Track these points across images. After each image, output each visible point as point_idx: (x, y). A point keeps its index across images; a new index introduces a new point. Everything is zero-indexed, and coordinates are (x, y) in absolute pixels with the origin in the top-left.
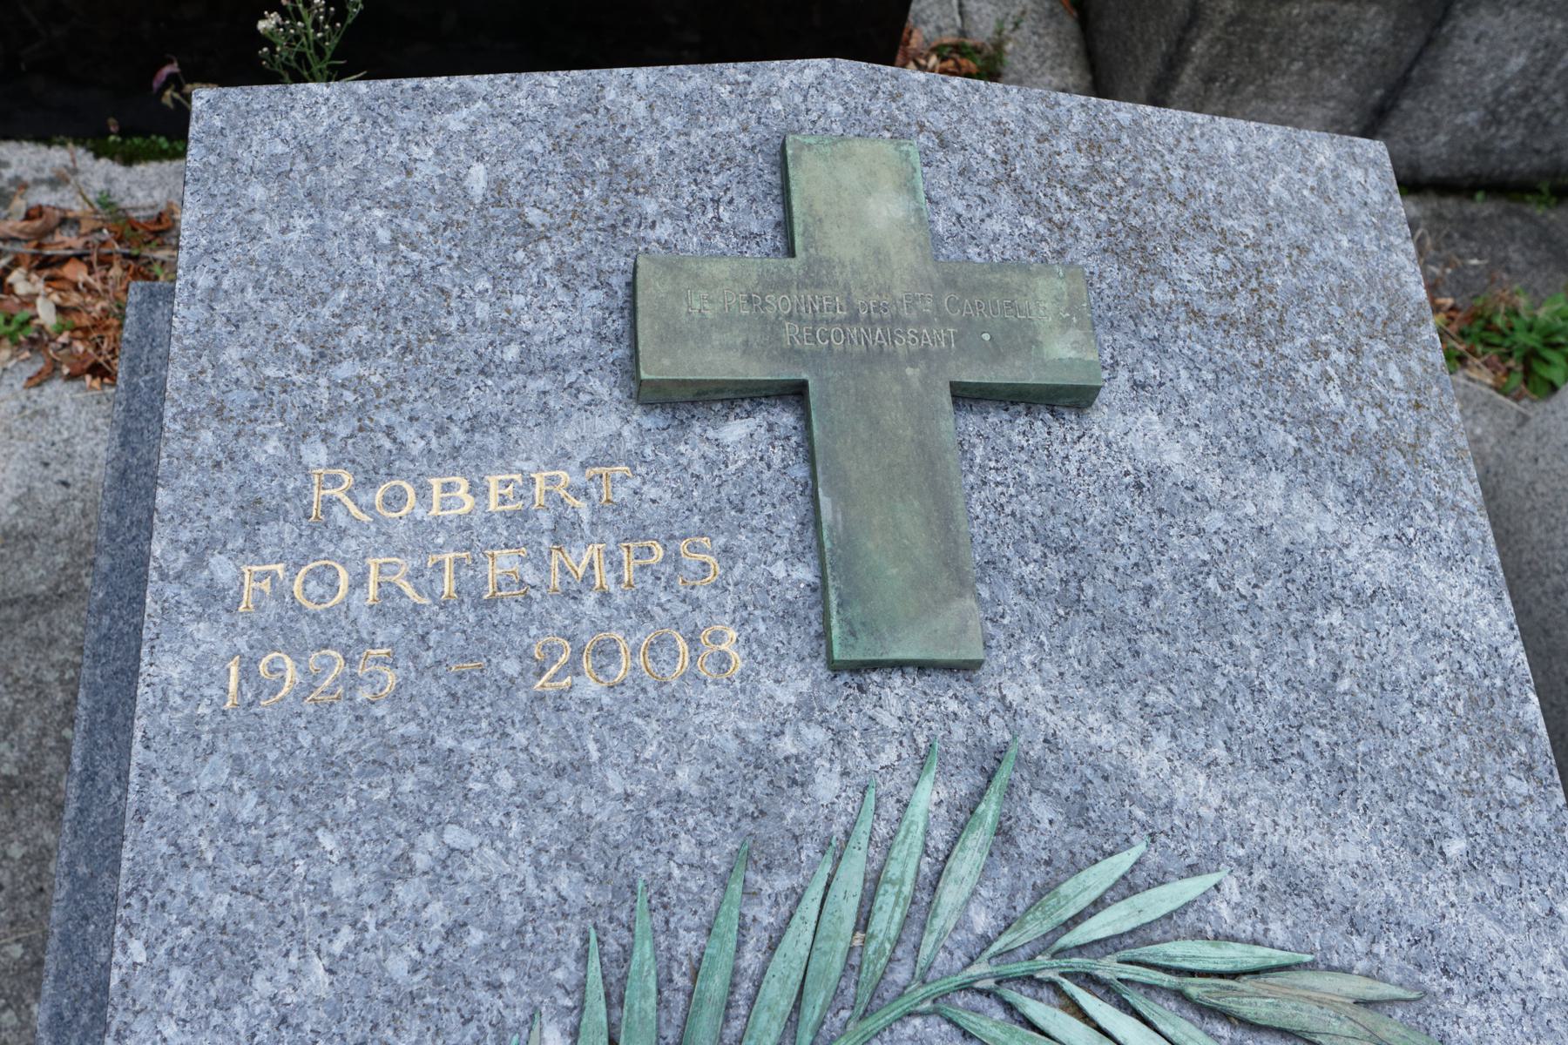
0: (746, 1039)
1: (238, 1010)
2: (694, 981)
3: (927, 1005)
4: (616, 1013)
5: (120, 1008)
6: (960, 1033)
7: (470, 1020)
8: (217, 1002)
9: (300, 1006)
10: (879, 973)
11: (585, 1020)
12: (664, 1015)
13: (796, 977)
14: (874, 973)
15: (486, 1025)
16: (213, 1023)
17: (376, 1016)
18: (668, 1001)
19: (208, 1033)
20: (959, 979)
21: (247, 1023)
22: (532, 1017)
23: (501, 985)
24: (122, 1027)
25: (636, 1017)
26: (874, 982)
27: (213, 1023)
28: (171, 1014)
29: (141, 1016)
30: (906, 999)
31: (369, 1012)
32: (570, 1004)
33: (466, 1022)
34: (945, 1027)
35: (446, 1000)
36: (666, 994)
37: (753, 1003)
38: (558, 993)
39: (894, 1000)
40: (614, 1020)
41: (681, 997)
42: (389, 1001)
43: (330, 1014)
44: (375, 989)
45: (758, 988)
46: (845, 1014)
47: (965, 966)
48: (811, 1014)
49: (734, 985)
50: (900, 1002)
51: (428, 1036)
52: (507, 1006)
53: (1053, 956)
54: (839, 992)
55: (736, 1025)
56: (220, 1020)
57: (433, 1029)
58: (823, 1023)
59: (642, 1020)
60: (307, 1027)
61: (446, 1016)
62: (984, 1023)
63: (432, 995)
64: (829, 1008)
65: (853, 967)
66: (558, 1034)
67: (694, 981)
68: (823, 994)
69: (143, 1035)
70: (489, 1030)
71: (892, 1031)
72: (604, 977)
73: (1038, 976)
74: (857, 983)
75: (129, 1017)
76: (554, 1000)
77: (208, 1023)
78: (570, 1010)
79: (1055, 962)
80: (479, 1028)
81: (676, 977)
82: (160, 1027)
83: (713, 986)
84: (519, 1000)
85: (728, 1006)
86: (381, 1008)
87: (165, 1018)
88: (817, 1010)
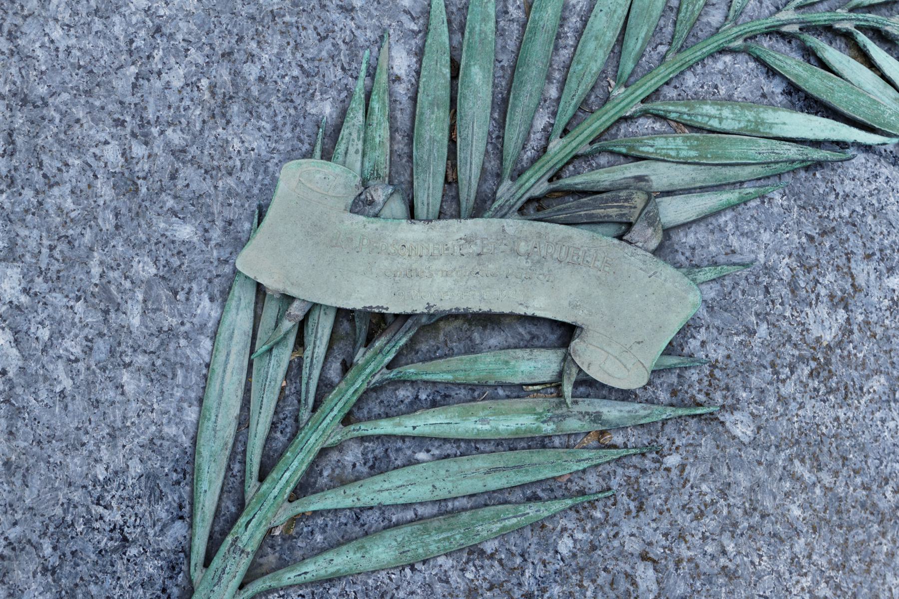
0: (574, 64)
1: (116, 19)
2: (527, 14)
3: (739, 43)
4: (457, 37)
5: (10, 12)
6: (764, 70)
7: (326, 37)
8: (97, 11)
9: (172, 18)
10: (697, 13)
11: (429, 41)
12: (500, 41)
13: (622, 12)
14: (693, 12)
15: (340, 42)
16: (94, 29)
17: (241, 30)
18: (503, 30)
19: (90, 38)
20: (770, 22)
21: (126, 31)
22: (382, 37)
23: (353, 9)
24: (13, 28)
25: (477, 38)
26: (692, 21)
27: (94, 29)
28: (56, 20)
29: (29, 20)
30: (721, 36)
31: (235, 26)
32: (416, 28)
33: (322, 39)
34: (752, 64)
35: (303, 19)
36: (502, 23)
37: (581, 34)
38: (405, 18)
39: (708, 38)
40: (455, 43)
41: (515, 26)
42: (253, 18)
43: (200, 27)
44: (240, 6)
45: (585, 23)
46: (662, 49)
47: (772, 14)
48: (634, 45)
49: (563, 19)
50: (716, 38)
51: (288, 50)
52: (358, 27)
53: (851, 10)
54: (659, 29)
55: (565, 53)
56: (101, 27)
57: (292, 43)
58: (643, 55)
59: (482, 41)
60: (180, 37)
61: (303, 33)
62: (789, 62)
63: (291, 14)
64: (649, 42)
65: (671, 9)
66: (404, 54)
67: (527, 14)
68: (645, 29)
69: (32, 36)
70: (343, 47)
71: (704, 66)
72: (446, 6)
73: (837, 26)
74: (675, 23)
75: (19, 21)
76: (401, 24)
77: (90, 29)
78: (415, 33)
79: (853, 15)
80: (333, 45)
81: (511, 9)
82: (47, 31)
83: (546, 16)
84: (367, 23)
85: (558, 37)
86: (245, 23)
87: (51, 23)
88: (640, 41)
